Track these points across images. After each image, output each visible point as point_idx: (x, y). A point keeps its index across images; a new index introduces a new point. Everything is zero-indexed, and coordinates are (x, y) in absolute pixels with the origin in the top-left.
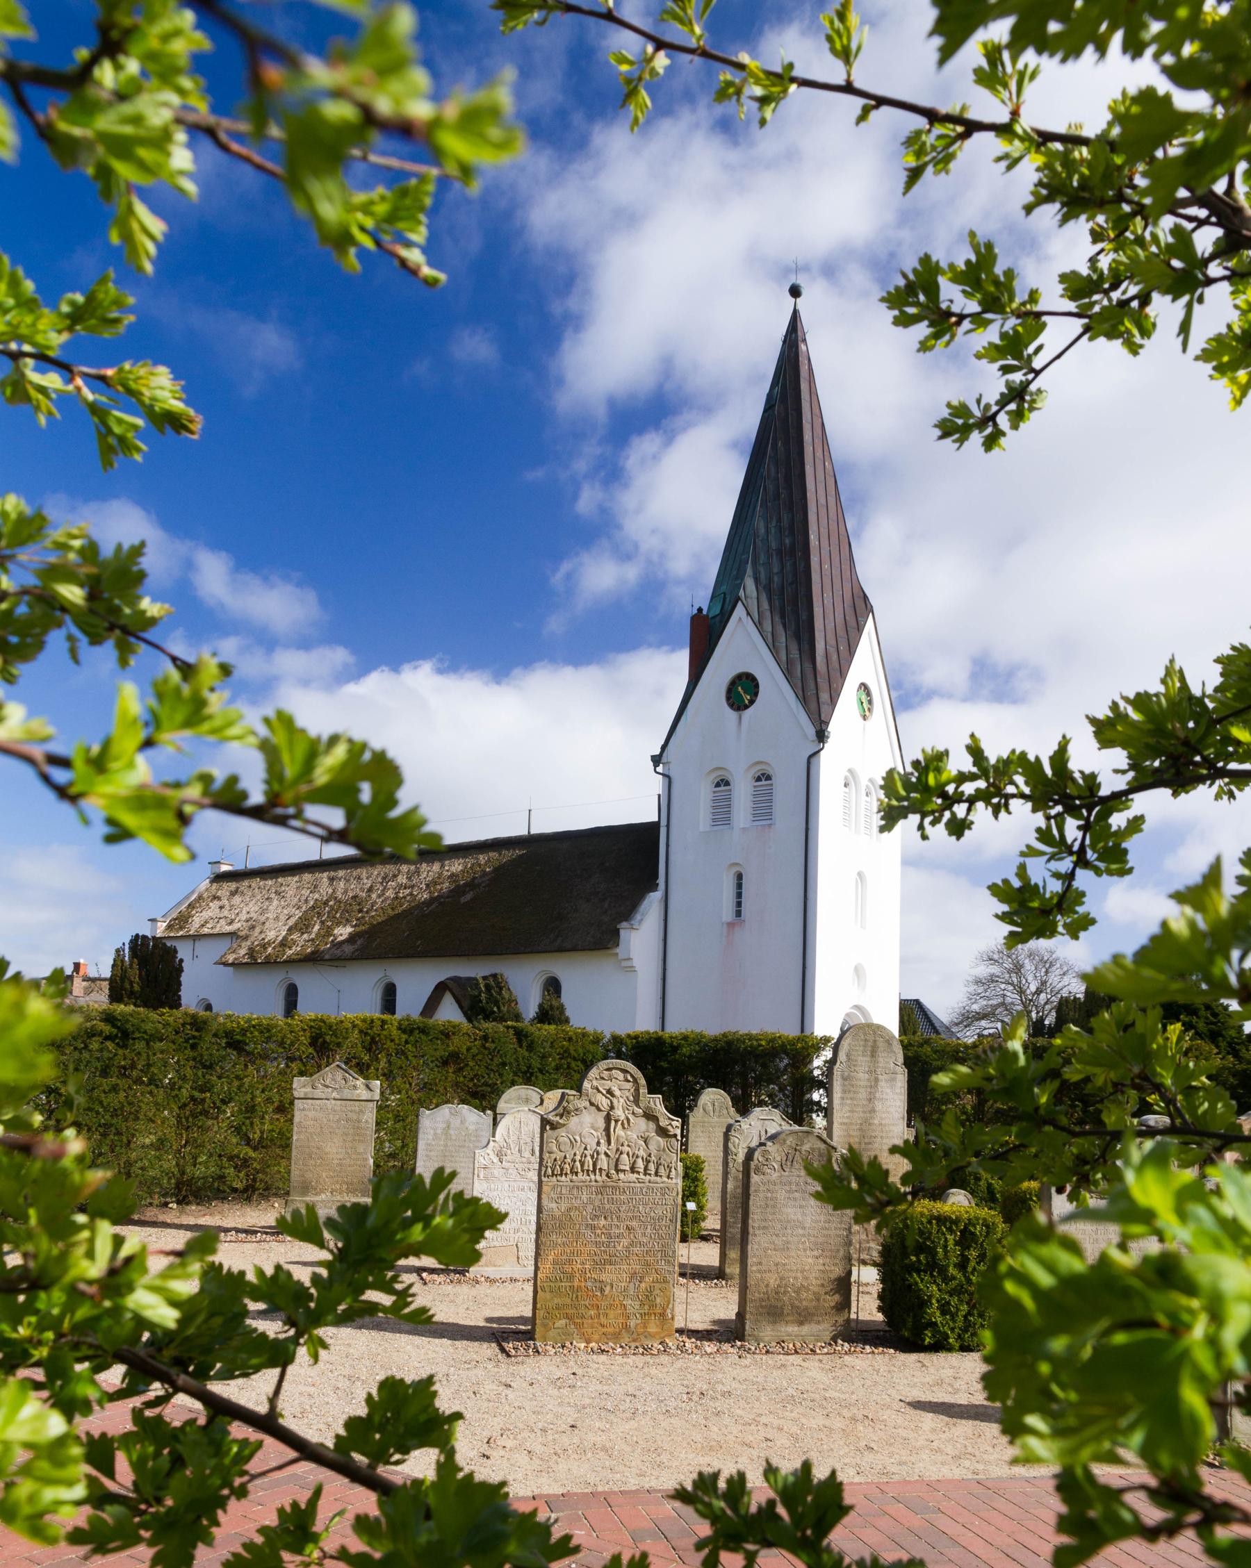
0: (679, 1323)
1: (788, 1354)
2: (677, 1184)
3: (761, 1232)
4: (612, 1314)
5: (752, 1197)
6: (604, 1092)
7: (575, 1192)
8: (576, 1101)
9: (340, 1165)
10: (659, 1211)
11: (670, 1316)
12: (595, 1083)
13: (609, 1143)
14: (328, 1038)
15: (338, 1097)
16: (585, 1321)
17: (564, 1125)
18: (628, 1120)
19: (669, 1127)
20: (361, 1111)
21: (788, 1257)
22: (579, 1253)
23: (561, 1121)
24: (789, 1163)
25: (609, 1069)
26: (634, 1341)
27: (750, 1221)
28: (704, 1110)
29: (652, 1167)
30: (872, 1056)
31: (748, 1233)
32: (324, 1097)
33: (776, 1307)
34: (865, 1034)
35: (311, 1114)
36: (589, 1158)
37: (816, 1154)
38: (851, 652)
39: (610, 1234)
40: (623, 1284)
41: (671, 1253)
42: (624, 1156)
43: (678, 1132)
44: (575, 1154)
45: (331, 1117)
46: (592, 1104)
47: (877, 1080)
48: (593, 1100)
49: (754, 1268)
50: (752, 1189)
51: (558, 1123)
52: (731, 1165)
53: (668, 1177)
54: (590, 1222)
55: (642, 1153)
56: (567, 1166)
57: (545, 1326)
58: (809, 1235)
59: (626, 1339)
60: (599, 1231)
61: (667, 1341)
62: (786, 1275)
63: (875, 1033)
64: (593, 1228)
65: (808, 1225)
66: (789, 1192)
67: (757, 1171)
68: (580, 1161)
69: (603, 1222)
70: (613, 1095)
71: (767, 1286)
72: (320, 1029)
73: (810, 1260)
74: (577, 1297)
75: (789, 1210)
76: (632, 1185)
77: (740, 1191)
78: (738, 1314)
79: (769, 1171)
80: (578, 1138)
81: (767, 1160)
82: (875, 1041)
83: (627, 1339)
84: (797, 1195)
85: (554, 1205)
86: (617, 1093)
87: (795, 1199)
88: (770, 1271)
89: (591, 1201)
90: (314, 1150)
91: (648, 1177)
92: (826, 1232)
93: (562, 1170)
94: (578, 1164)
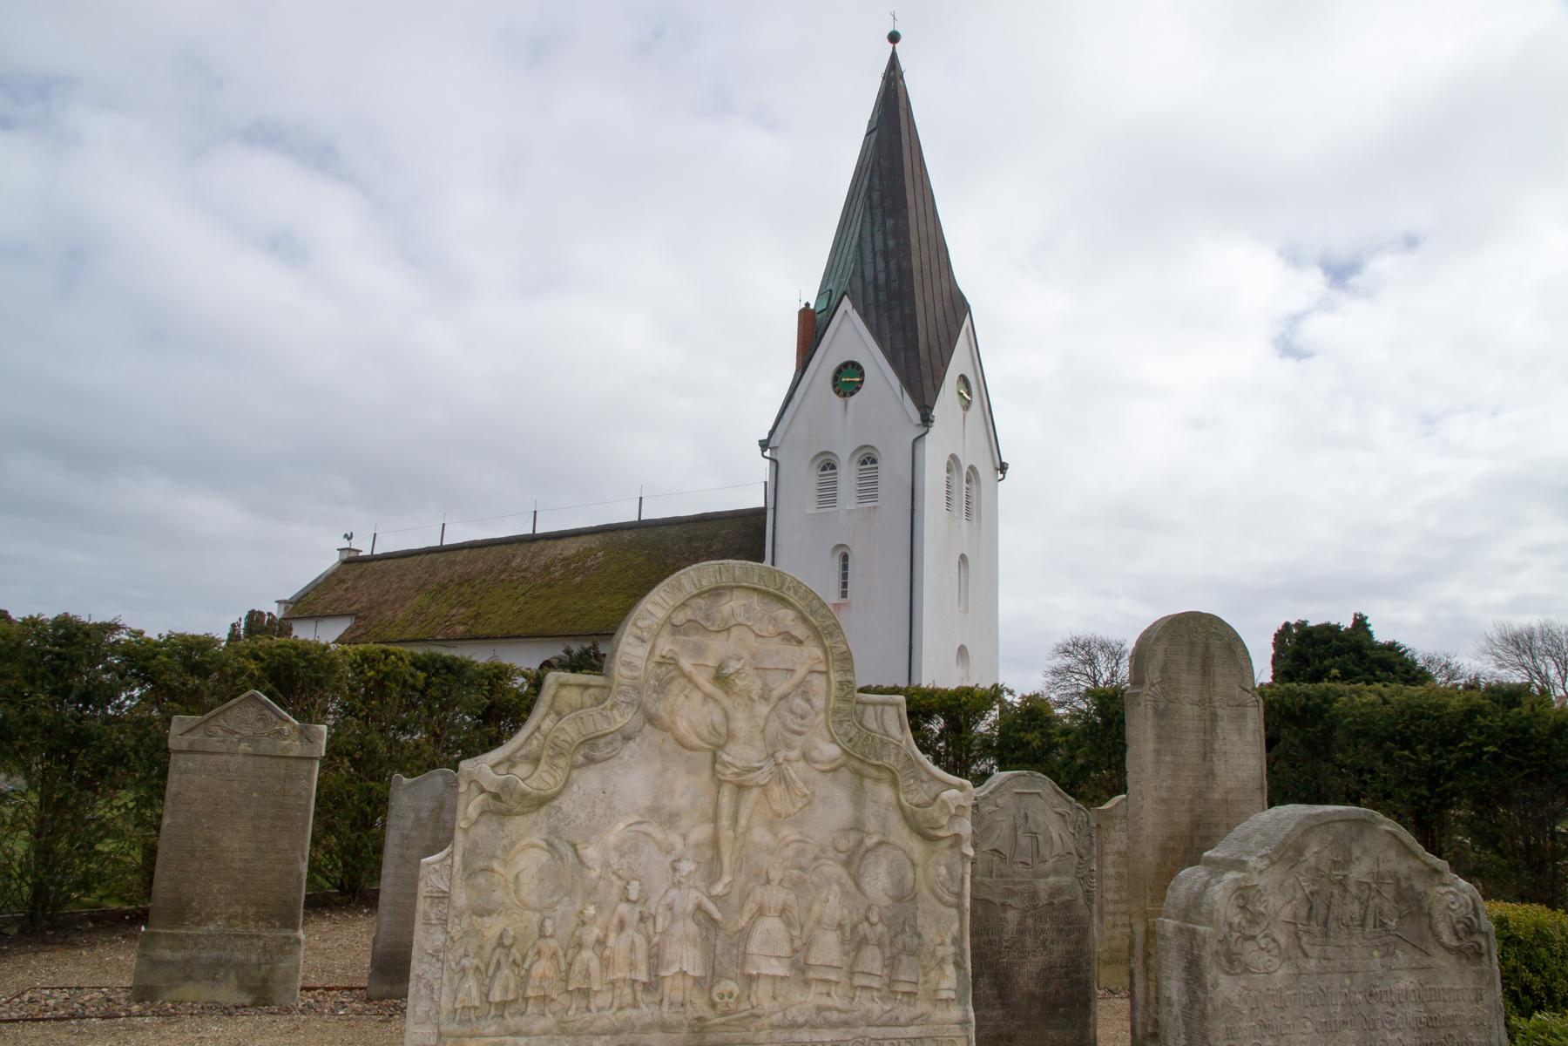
17: (542, 801)
25: (716, 592)
32: (224, 748)
45: (236, 785)
46: (651, 719)
48: (661, 708)
86: (748, 682)
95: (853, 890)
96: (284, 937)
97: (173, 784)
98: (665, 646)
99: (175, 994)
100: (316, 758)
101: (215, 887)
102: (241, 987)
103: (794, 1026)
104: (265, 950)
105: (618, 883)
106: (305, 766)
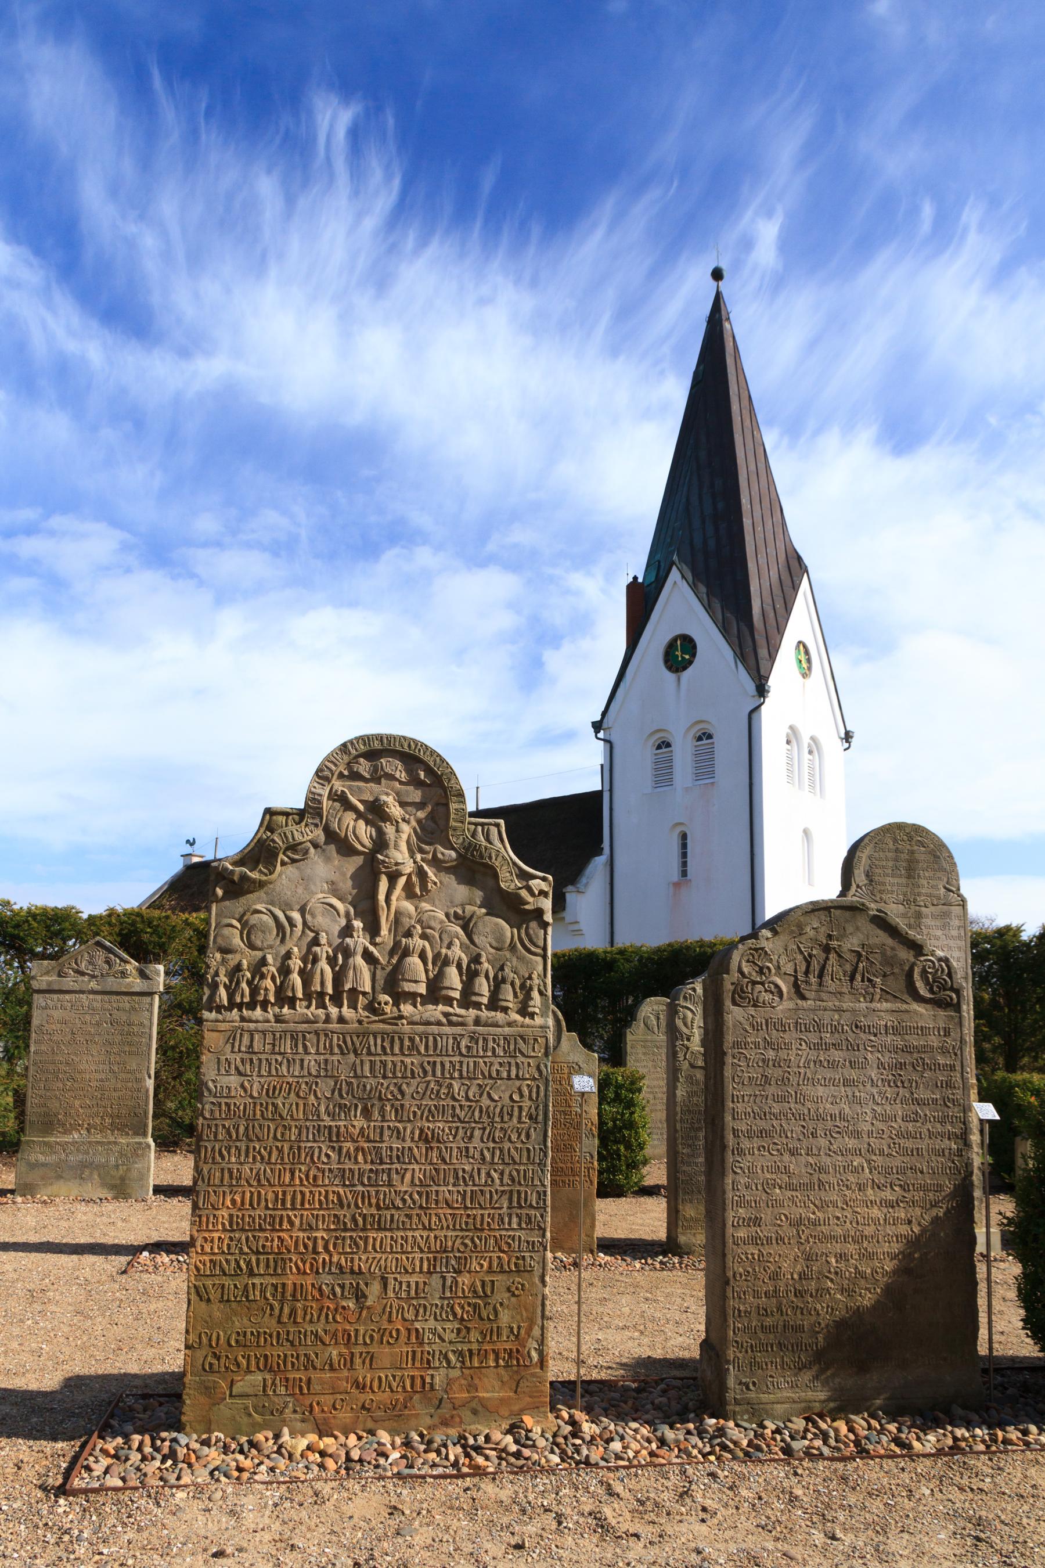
0: (559, 1370)
1: (843, 1459)
2: (544, 1027)
3: (756, 1142)
4: (385, 1354)
5: (729, 1060)
6: (361, 807)
7: (287, 1046)
8: (293, 828)
9: (101, 1089)
10: (502, 1093)
11: (534, 1355)
12: (338, 786)
13: (373, 929)
14: (145, 937)
15: (99, 988)
16: (314, 1375)
17: (261, 885)
18: (422, 874)
19: (524, 893)
20: (134, 1009)
21: (822, 1206)
22: (299, 1203)
23: (254, 875)
24: (813, 980)
26: (445, 1423)
27: (728, 1118)
28: (646, 1024)
29: (483, 987)
30: (909, 877)
31: (724, 1147)
32: (77, 987)
33: (799, 1329)
34: (895, 840)
35: (57, 1014)
36: (323, 965)
37: (876, 959)
38: (788, 609)
39: (378, 1150)
40: (413, 1279)
41: (533, 1199)
42: (415, 960)
43: (547, 904)
44: (288, 955)
47: (919, 915)
49: (741, 1233)
50: (729, 1038)
51: (244, 877)
52: (681, 1056)
53: (524, 1011)
54: (328, 1121)
55: (457, 952)
56: (268, 983)
57: (208, 1390)
58: (870, 1150)
59: (423, 1416)
60: (349, 1146)
61: (528, 1421)
62: (820, 1248)
63: (910, 839)
64: (334, 1137)
65: (865, 1127)
66: (817, 1047)
67: (740, 996)
68: (302, 972)
69: (360, 1123)
70: (386, 817)
71: (775, 1276)
72: (133, 924)
73: (876, 1212)
74: (293, 1312)
75: (821, 1091)
76: (435, 1029)
77: (700, 1100)
78: (705, 1345)
79: (768, 997)
80: (296, 916)
81: (761, 972)
82: (912, 852)
83: (428, 1421)
84: (837, 1055)
85: (233, 1081)
86: (395, 810)
87: (833, 1065)
88: (780, 1239)
89: (326, 1070)
90: (62, 1067)
91: (473, 1012)
92: (909, 1144)
93: (254, 991)
94: (296, 979)
95: (468, 942)
96: (136, 1143)
97: (37, 1019)
98: (338, 786)
99: (49, 1190)
100: (155, 993)
101: (77, 1103)
102: (104, 1185)
103: (428, 1023)
104: (121, 1154)
105: (312, 935)
106: (148, 999)
